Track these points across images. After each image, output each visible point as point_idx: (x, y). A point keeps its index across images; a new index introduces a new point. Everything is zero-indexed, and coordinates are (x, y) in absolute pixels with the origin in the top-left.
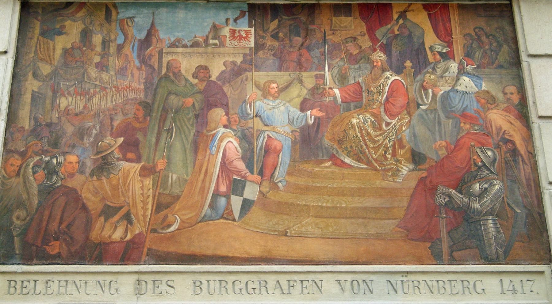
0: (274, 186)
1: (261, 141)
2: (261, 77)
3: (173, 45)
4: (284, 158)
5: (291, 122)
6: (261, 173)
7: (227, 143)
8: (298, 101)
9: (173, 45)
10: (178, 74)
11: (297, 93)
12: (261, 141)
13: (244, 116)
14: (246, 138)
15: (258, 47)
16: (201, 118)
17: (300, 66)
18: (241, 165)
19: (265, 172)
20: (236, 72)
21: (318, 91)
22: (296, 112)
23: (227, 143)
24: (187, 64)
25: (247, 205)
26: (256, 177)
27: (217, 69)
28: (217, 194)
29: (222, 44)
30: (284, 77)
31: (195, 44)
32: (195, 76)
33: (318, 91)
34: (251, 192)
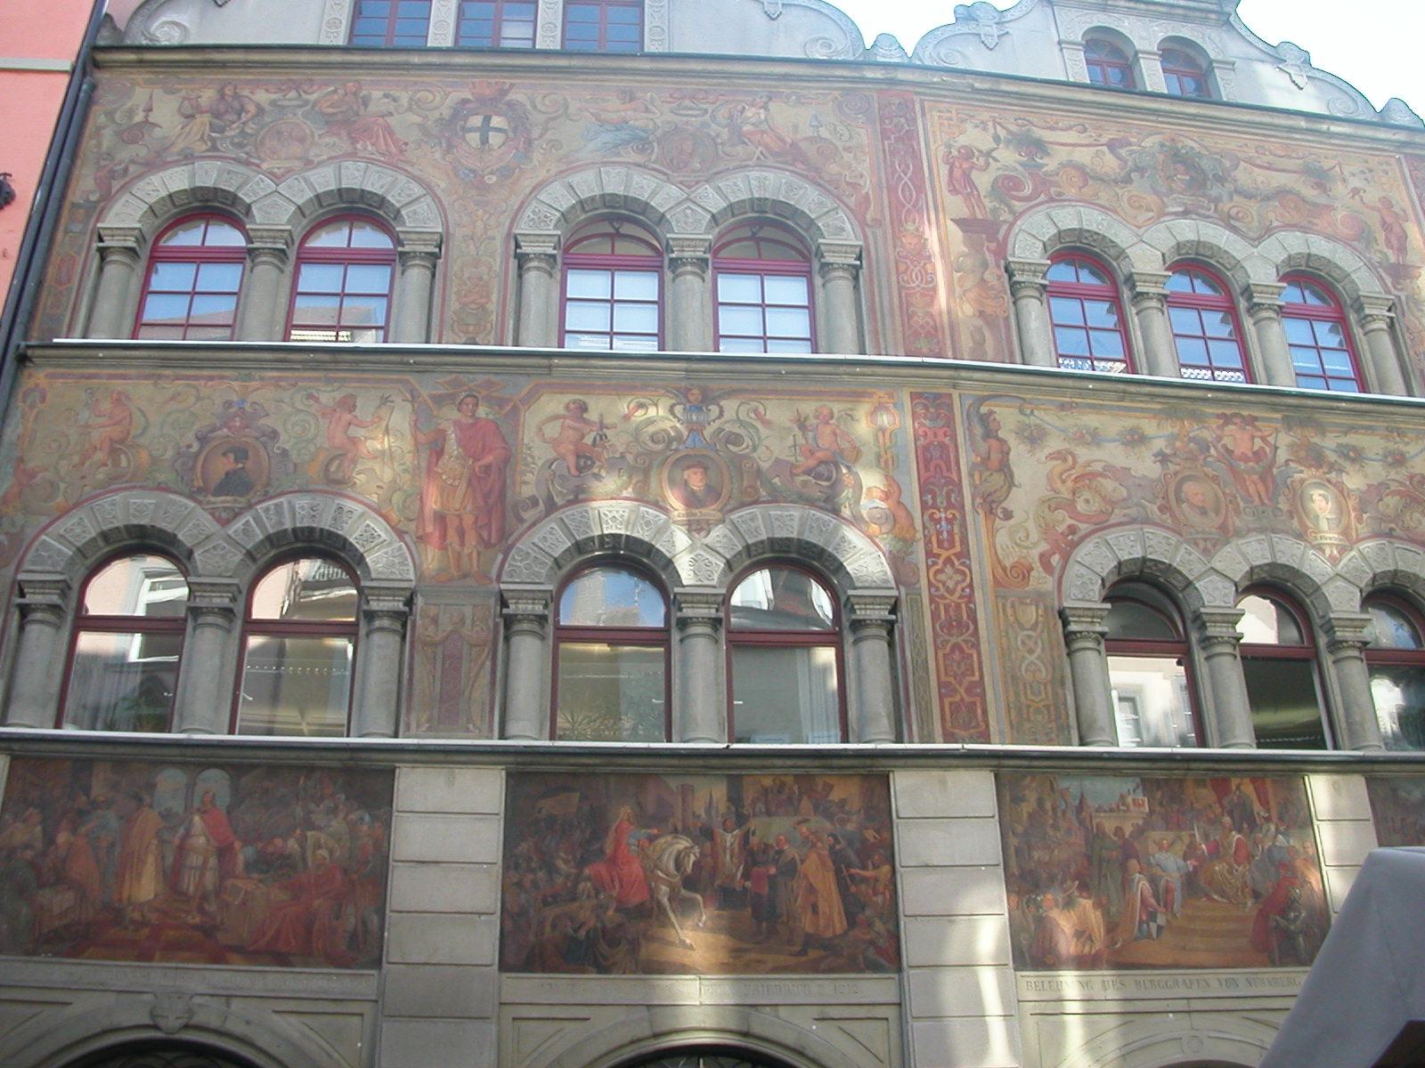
0: (1174, 915)
1: (1163, 883)
2: (1155, 835)
3: (1098, 810)
4: (1178, 896)
5: (1178, 869)
6: (1165, 906)
7: (1142, 885)
8: (1181, 853)
9: (1098, 810)
10: (1104, 833)
11: (1180, 847)
12: (1163, 883)
13: (1149, 864)
14: (1153, 881)
15: (1152, 812)
16: (1123, 866)
17: (1179, 827)
18: (1152, 901)
19: (1168, 905)
20: (1140, 832)
21: (1192, 847)
22: (1181, 862)
23: (1142, 885)
24: (1109, 825)
25: (1160, 928)
26: (1162, 909)
27: (1128, 830)
28: (1141, 922)
29: (1128, 810)
30: (1170, 835)
31: (1111, 810)
32: (1115, 834)
33: (1192, 847)
34: (1161, 920)
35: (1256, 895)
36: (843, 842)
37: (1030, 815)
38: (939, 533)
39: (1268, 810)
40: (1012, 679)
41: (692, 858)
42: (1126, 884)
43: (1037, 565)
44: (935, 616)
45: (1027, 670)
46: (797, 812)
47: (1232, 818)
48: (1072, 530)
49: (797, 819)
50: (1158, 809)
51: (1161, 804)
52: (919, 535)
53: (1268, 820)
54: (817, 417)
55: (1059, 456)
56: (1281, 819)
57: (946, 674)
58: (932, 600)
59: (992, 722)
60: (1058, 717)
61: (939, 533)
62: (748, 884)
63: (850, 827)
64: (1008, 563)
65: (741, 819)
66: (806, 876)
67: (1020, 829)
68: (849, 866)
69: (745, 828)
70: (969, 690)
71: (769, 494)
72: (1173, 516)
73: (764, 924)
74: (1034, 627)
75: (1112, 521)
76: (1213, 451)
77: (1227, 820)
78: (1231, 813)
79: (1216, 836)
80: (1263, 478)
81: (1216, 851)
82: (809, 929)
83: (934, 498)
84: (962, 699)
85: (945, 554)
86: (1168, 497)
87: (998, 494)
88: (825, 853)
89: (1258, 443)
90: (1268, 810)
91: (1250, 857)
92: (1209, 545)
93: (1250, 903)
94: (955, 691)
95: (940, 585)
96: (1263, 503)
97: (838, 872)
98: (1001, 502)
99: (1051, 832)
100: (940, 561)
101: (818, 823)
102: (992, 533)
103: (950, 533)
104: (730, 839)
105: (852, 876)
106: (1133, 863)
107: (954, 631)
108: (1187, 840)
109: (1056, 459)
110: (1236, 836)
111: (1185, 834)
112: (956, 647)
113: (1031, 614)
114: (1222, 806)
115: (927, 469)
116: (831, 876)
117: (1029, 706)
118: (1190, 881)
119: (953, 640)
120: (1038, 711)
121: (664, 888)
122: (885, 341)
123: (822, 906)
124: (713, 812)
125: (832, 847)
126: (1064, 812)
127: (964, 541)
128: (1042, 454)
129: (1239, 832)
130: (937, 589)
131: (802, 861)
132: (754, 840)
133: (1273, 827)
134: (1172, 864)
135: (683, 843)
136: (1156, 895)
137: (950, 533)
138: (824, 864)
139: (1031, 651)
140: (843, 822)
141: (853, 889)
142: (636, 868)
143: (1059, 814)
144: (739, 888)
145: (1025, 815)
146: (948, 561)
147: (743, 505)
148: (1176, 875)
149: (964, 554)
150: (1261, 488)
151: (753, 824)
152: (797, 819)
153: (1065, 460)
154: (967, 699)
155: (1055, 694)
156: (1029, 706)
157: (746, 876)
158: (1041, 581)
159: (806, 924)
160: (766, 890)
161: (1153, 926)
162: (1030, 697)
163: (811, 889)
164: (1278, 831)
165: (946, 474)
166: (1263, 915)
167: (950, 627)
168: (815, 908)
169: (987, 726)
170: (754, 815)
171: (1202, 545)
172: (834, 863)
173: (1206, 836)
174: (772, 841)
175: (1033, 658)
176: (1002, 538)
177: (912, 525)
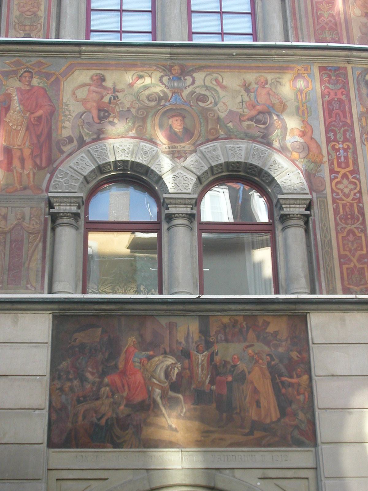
36: (277, 361)
38: (338, 158)
44: (336, 212)
46: (245, 340)
52: (325, 159)
54: (257, 83)
57: (344, 250)
58: (334, 201)
61: (338, 158)
62: (213, 387)
63: (281, 350)
65: (208, 345)
68: (280, 375)
69: (211, 350)
71: (226, 134)
73: (225, 414)
82: (255, 417)
84: (355, 266)
85: (342, 171)
88: (265, 367)
94: (350, 260)
95: (340, 192)
97: (273, 380)
100: (340, 176)
101: (259, 347)
103: (346, 158)
104: (201, 358)
105: (283, 383)
112: (351, 232)
115: (330, 117)
116: (268, 382)
119: (349, 227)
122: (302, 33)
124: (190, 340)
125: (269, 363)
131: (249, 372)
132: (217, 359)
137: (346, 158)
140: (276, 346)
146: (345, 176)
151: (217, 348)
154: (359, 266)
157: (212, 382)
159: (253, 414)
160: (225, 392)
163: (256, 391)
165: (343, 119)
167: (346, 219)
170: (217, 342)
172: (271, 373)
174: (229, 359)
177: (321, 153)
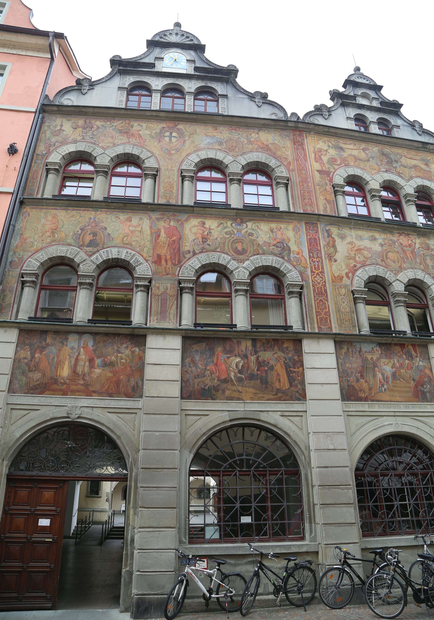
0: (389, 385)
1: (386, 375)
4: (390, 379)
6: (387, 383)
7: (379, 376)
8: (391, 366)
10: (367, 359)
11: (391, 364)
12: (386, 375)
14: (383, 375)
18: (383, 381)
19: (387, 382)
20: (378, 359)
23: (379, 376)
24: (369, 357)
27: (375, 358)
28: (379, 387)
29: (374, 352)
30: (387, 361)
34: (386, 387)
35: (414, 380)
36: (288, 360)
37: (345, 353)
38: (315, 265)
39: (417, 354)
40: (338, 311)
41: (241, 364)
42: (375, 376)
43: (345, 276)
44: (314, 291)
45: (343, 308)
47: (406, 356)
48: (355, 266)
49: (274, 352)
50: (383, 352)
51: (384, 351)
53: (417, 357)
55: (351, 243)
56: (420, 357)
57: (318, 309)
59: (333, 325)
60: (352, 323)
64: (336, 275)
66: (276, 370)
67: (342, 357)
68: (290, 367)
69: (257, 355)
70: (325, 314)
72: (385, 263)
74: (344, 295)
75: (367, 264)
76: (396, 244)
77: (404, 356)
78: (405, 354)
79: (401, 361)
80: (412, 253)
81: (401, 366)
83: (313, 255)
86: (384, 257)
87: (333, 254)
89: (410, 242)
90: (417, 354)
91: (412, 368)
92: (396, 272)
93: (412, 382)
96: (412, 260)
98: (333, 257)
99: (351, 358)
100: (315, 274)
102: (331, 266)
103: (318, 265)
105: (291, 371)
106: (376, 369)
107: (320, 295)
108: (392, 362)
109: (349, 244)
110: (407, 361)
111: (392, 360)
113: (343, 291)
114: (403, 352)
116: (284, 371)
117: (343, 319)
118: (394, 375)
119: (320, 298)
120: (346, 321)
121: (233, 374)
123: (282, 379)
124: (247, 350)
125: (284, 361)
126: (355, 352)
127: (323, 268)
128: (345, 242)
129: (408, 360)
130: (315, 283)
131: (275, 366)
133: (418, 359)
134: (388, 369)
135: (238, 359)
136: (384, 379)
137: (318, 265)
138: (282, 367)
139: (344, 303)
140: (288, 354)
141: (291, 375)
142: (224, 367)
143: (354, 353)
144: (256, 374)
145: (343, 353)
146: (318, 274)
147: (254, 255)
148: (390, 373)
149: (322, 272)
150: (411, 255)
152: (274, 352)
153: (352, 245)
155: (351, 316)
156: (343, 319)
157: (258, 370)
158: (346, 281)
160: (264, 375)
161: (383, 389)
162: (344, 316)
163: (278, 375)
164: (420, 360)
166: (416, 386)
167: (319, 294)
168: (279, 380)
169: (331, 325)
170: (260, 351)
171: (394, 272)
172: (285, 366)
173: (398, 361)
174: (266, 359)
175: (344, 304)
176: (334, 268)
